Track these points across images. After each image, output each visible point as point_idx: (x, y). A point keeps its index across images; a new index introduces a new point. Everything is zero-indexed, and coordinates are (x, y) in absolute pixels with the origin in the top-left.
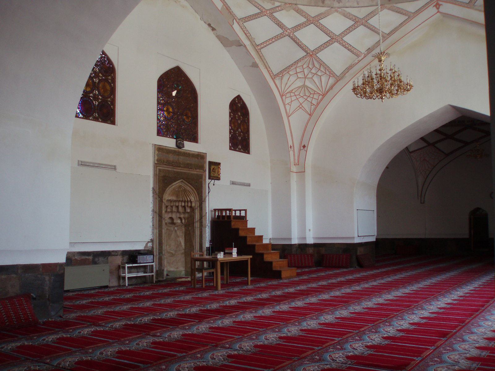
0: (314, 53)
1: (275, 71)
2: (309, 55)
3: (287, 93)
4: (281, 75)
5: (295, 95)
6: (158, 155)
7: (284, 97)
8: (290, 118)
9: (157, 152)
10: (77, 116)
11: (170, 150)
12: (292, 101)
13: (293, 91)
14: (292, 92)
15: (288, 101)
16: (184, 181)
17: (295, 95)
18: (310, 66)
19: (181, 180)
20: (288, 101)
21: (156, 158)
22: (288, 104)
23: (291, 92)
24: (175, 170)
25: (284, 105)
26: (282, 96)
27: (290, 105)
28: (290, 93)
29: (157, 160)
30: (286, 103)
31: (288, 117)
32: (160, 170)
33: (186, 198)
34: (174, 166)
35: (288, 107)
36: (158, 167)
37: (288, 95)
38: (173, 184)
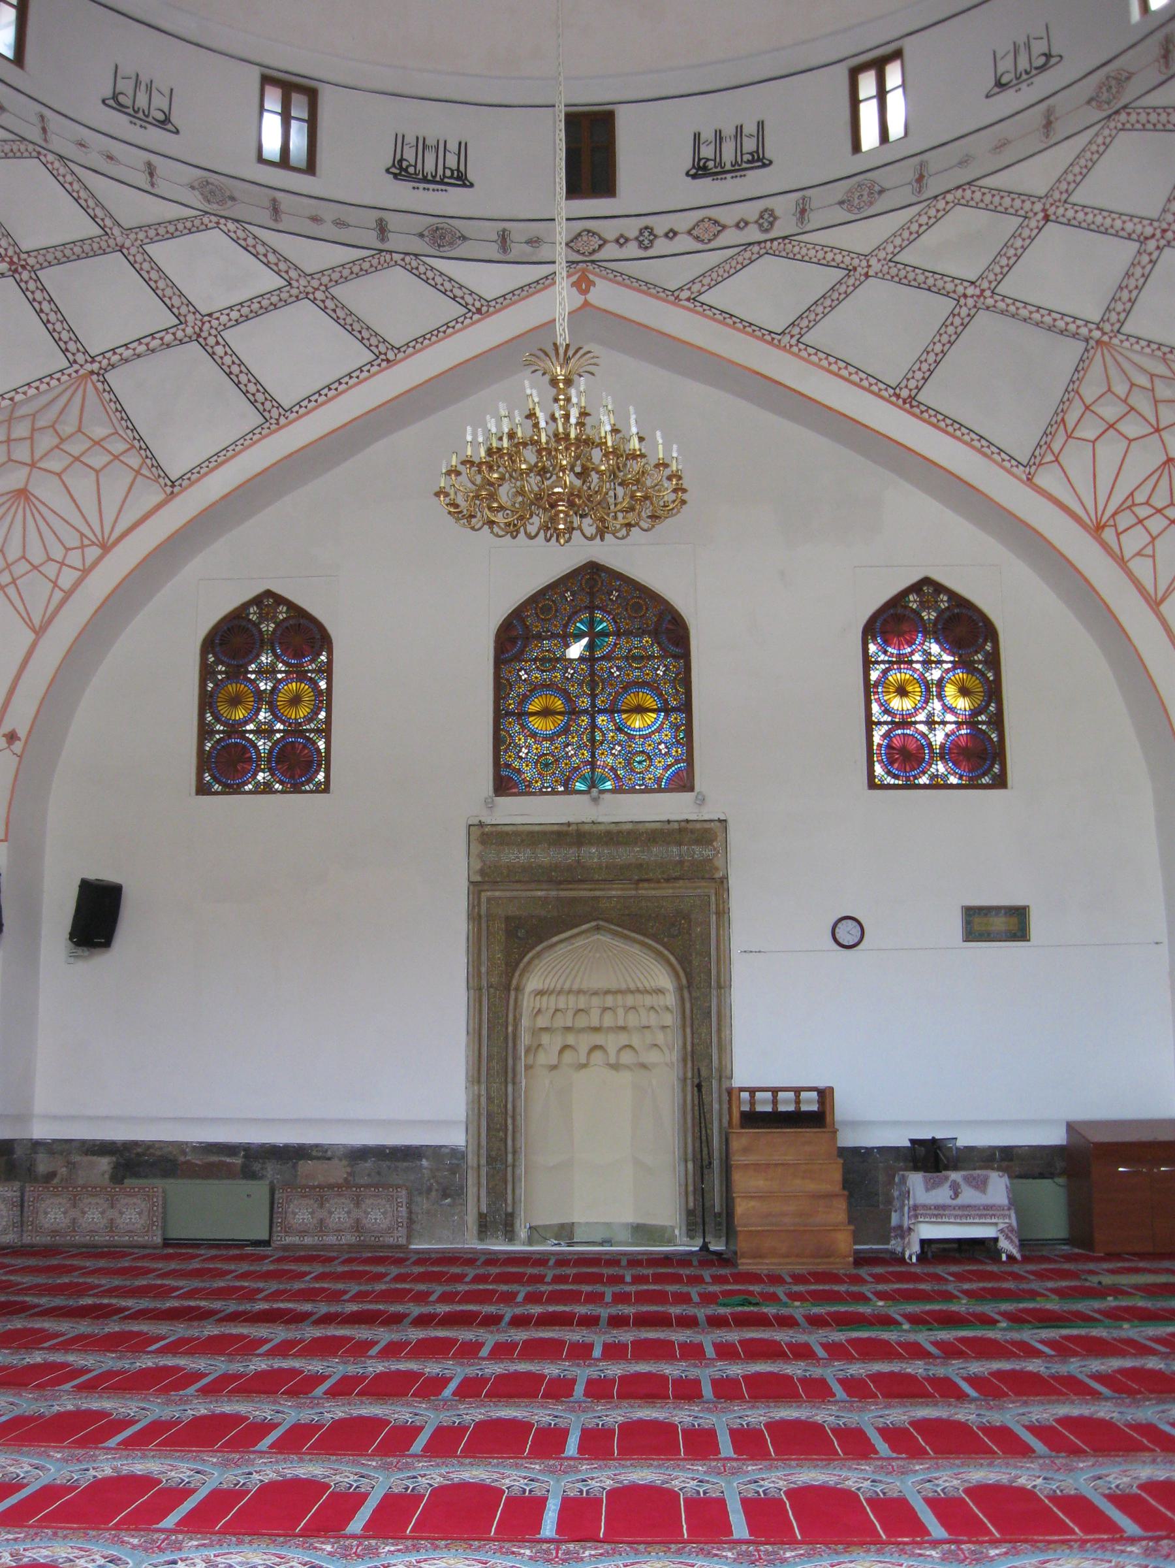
0: (1107, 327)
1: (1021, 446)
2: (1092, 343)
3: (1114, 515)
4: (1049, 457)
5: (1159, 511)
6: (480, 856)
7: (1109, 535)
8: (1164, 608)
9: (476, 848)
10: (325, 788)
11: (538, 832)
12: (1153, 539)
13: (1140, 498)
14: (1134, 504)
15: (1133, 542)
16: (601, 923)
17: (1159, 511)
18: (1143, 381)
19: (593, 924)
20: (1133, 542)
21: (478, 865)
22: (1139, 554)
23: (1129, 504)
24: (563, 894)
25: (1122, 562)
26: (1097, 530)
27: (1153, 557)
28: (1129, 507)
29: (482, 872)
30: (1127, 556)
31: (1155, 604)
32: (489, 900)
33: (629, 979)
34: (560, 883)
35: (1141, 568)
36: (483, 894)
37: (1125, 520)
38: (555, 939)
